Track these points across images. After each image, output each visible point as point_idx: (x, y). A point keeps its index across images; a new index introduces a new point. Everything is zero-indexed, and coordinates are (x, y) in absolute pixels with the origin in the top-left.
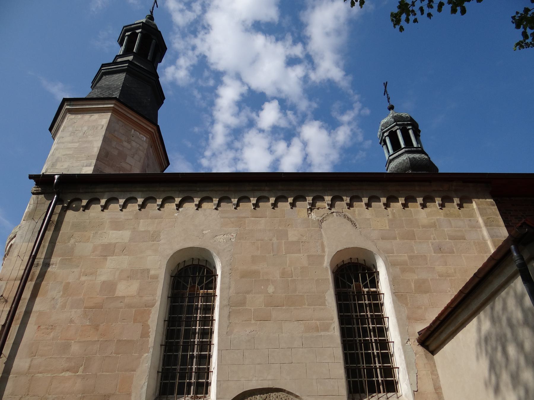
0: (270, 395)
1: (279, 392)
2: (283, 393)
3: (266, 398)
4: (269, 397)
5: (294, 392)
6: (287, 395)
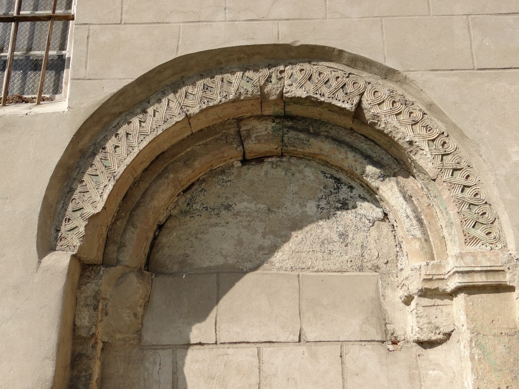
0: (282, 72)
1: (318, 61)
3: (269, 80)
4: (280, 79)
5: (378, 59)
6: (348, 70)
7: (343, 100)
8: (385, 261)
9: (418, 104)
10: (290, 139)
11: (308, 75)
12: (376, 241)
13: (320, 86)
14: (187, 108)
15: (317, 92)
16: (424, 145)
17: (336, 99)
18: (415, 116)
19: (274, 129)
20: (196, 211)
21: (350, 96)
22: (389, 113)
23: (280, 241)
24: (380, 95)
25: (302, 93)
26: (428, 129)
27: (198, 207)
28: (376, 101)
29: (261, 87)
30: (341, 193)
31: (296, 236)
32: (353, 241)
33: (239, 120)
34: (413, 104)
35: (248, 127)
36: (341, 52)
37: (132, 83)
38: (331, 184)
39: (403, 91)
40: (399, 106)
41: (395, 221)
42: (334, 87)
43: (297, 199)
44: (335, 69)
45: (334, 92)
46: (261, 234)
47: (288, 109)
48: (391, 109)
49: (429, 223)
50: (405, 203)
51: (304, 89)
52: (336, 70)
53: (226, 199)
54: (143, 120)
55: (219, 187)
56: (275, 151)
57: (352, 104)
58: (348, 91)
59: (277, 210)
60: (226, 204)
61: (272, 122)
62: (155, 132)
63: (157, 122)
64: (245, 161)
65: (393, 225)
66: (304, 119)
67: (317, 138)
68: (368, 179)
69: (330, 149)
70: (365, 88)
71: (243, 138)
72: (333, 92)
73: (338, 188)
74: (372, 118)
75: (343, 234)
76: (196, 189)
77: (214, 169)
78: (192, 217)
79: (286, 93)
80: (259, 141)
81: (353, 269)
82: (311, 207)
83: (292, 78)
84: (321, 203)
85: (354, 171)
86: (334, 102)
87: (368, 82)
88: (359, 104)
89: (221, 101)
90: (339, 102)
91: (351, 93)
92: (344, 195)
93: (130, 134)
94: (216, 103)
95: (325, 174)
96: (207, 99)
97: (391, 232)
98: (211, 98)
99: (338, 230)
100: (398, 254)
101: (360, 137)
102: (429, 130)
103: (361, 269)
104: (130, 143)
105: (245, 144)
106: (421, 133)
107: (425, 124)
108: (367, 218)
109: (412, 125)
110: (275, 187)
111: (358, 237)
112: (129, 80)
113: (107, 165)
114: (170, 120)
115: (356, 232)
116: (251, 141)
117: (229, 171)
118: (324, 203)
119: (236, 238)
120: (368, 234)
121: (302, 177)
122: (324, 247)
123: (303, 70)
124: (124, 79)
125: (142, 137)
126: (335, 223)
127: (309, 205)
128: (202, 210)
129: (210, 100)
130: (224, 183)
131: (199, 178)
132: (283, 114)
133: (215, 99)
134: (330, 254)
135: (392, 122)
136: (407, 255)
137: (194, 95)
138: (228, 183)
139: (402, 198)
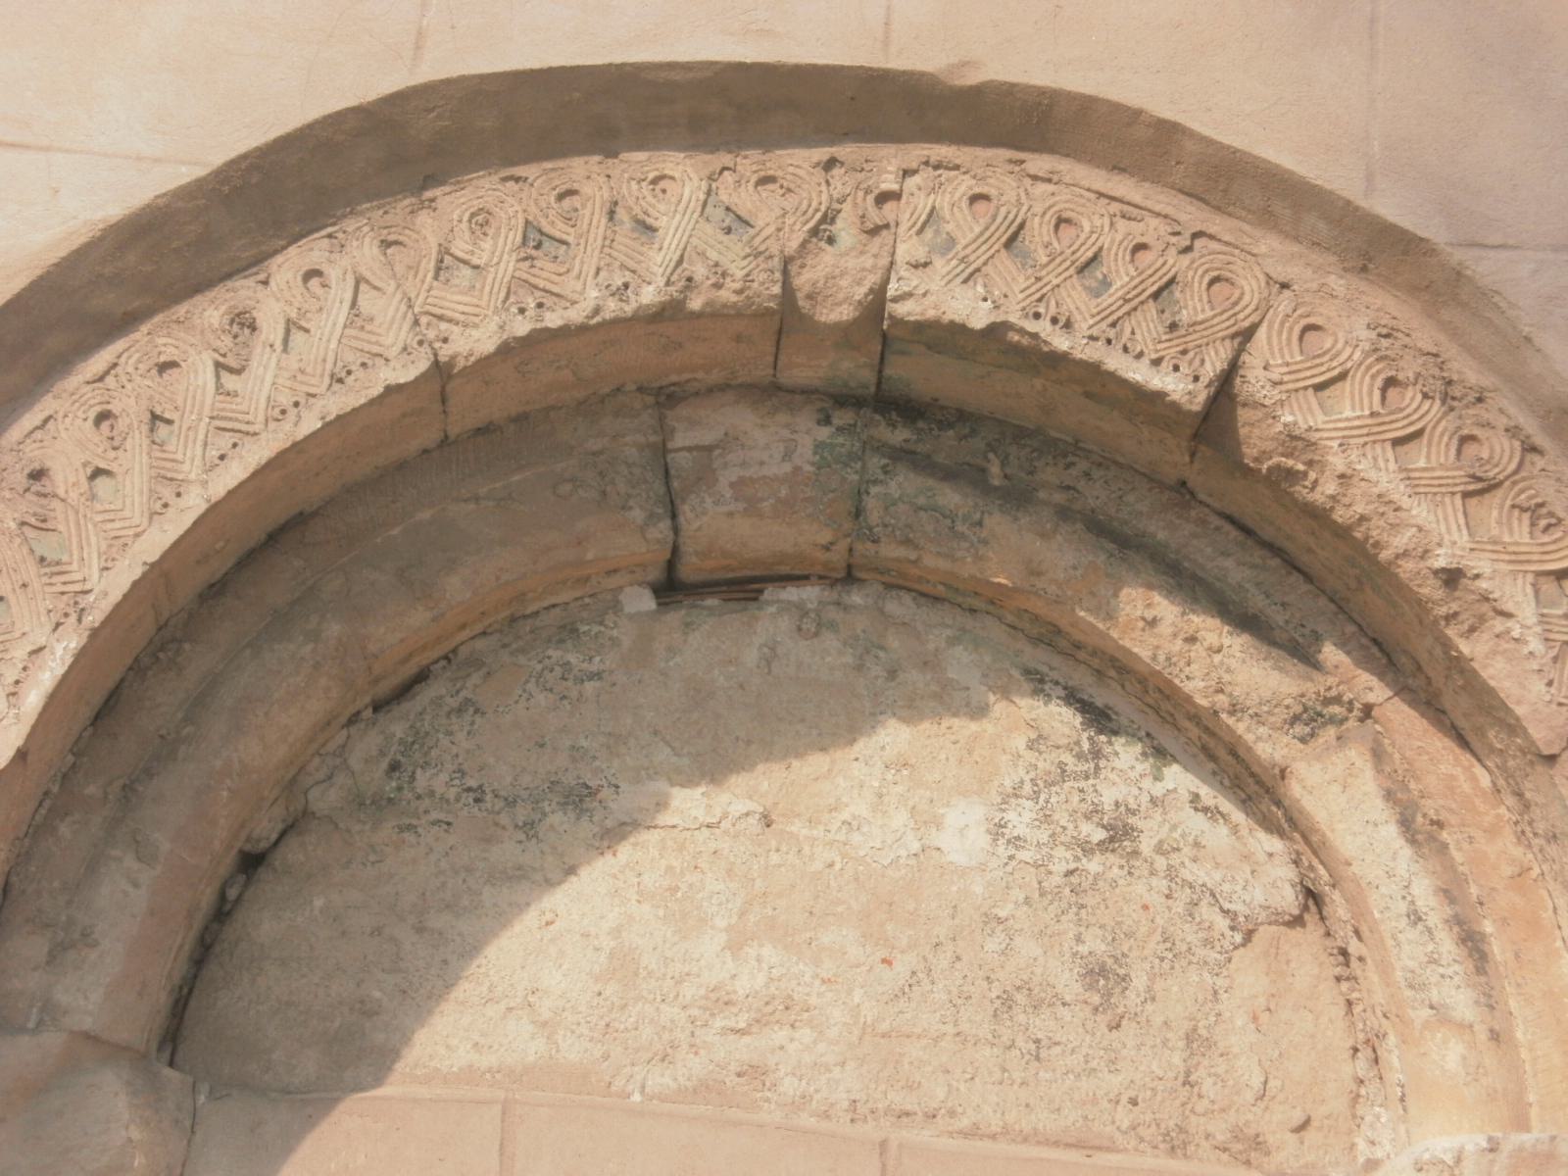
2: (1123, 186)
3: (822, 231)
6: (1192, 215)
7: (1154, 356)
8: (1298, 1117)
9: (1505, 403)
10: (892, 509)
11: (1007, 223)
12: (1255, 1019)
13: (1055, 282)
14: (444, 326)
15: (1042, 310)
16: (1518, 597)
17: (1125, 349)
18: (1485, 455)
19: (822, 458)
20: (427, 801)
21: (1189, 338)
22: (1365, 431)
23: (807, 978)
24: (1328, 345)
25: (971, 309)
26: (1543, 523)
27: (439, 783)
28: (1308, 373)
29: (787, 262)
30: (1112, 776)
31: (884, 961)
32: (1149, 1007)
33: (667, 398)
34: (1480, 400)
35: (707, 437)
36: (1168, 131)
37: (199, 183)
38: (1067, 731)
39: (1442, 338)
40: (1414, 405)
41: (1357, 932)
42: (1120, 293)
43: (899, 789)
44: (1131, 209)
45: (1120, 313)
46: (723, 938)
47: (900, 370)
48: (1373, 414)
49: (1517, 956)
50: (1407, 852)
51: (980, 289)
52: (1135, 212)
53: (574, 760)
54: (232, 361)
55: (542, 699)
56: (822, 556)
57: (1196, 379)
58: (1185, 316)
59: (804, 832)
60: (569, 779)
61: (819, 423)
62: (287, 426)
63: (300, 377)
64: (671, 588)
65: (1344, 953)
66: (963, 418)
67: (1020, 515)
68: (1240, 728)
69: (1072, 572)
70: (1264, 308)
71: (676, 484)
72: (1114, 317)
73: (1097, 754)
74: (1280, 449)
75: (1104, 971)
76: (437, 702)
77: (528, 612)
78: (410, 827)
79: (895, 300)
80: (752, 508)
81: (1142, 1140)
82: (962, 831)
83: (929, 233)
84: (1011, 816)
85: (1177, 681)
86: (1115, 362)
87: (1281, 279)
88: (1225, 387)
89: (597, 311)
90: (1135, 364)
91: (1195, 324)
92: (1124, 789)
93: (169, 422)
94: (576, 315)
95: (1042, 681)
96: (538, 294)
97: (1332, 982)
98: (556, 289)
99: (1083, 949)
100: (1363, 1092)
101: (1217, 529)
102: (1547, 528)
103: (1177, 1144)
104: (169, 465)
105: (685, 510)
106: (1507, 539)
107: (1531, 498)
108: (1221, 908)
109: (1466, 495)
110: (803, 720)
111: (1175, 989)
112: (183, 169)
113: (50, 556)
114: (359, 373)
115: (1166, 965)
116: (716, 503)
117: (596, 629)
118: (1028, 816)
119: (608, 944)
120: (1220, 982)
121: (934, 688)
122: (1008, 1023)
123: (985, 197)
124: (157, 161)
125: (225, 442)
126: (1071, 916)
127: (953, 817)
128: (457, 800)
129: (548, 301)
130: (570, 683)
131: (454, 651)
132: (873, 389)
133: (575, 297)
134: (1038, 1058)
135: (1372, 475)
136: (1402, 1100)
137: (476, 267)
138: (590, 687)
139: (1391, 831)
